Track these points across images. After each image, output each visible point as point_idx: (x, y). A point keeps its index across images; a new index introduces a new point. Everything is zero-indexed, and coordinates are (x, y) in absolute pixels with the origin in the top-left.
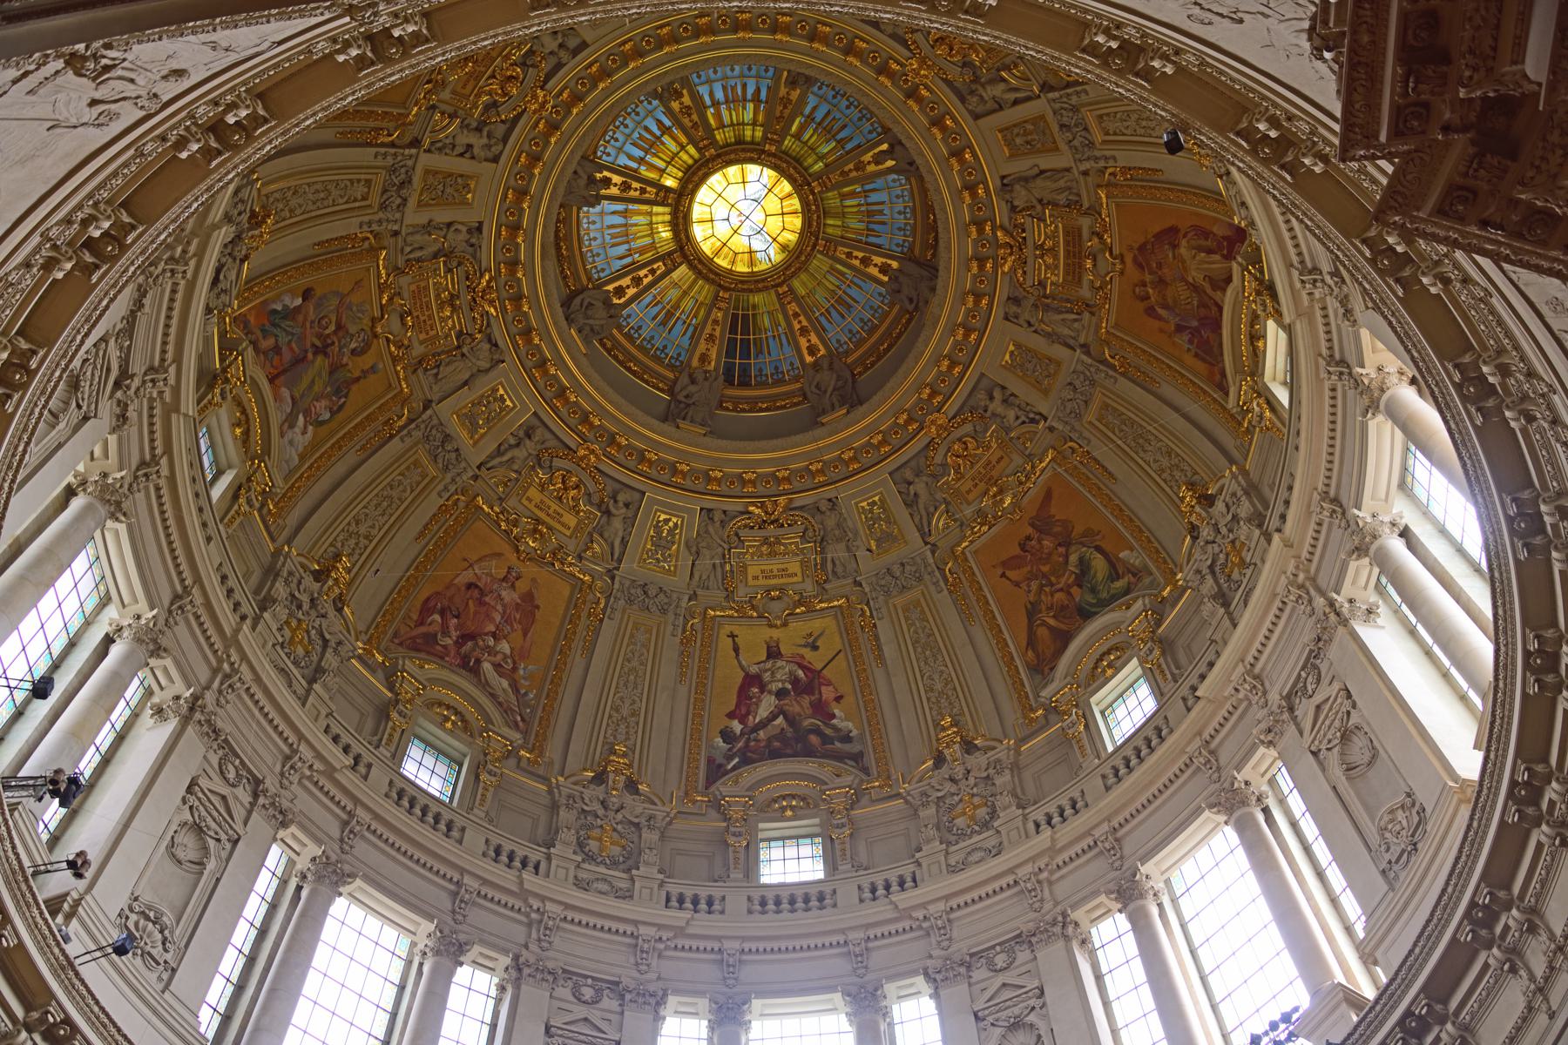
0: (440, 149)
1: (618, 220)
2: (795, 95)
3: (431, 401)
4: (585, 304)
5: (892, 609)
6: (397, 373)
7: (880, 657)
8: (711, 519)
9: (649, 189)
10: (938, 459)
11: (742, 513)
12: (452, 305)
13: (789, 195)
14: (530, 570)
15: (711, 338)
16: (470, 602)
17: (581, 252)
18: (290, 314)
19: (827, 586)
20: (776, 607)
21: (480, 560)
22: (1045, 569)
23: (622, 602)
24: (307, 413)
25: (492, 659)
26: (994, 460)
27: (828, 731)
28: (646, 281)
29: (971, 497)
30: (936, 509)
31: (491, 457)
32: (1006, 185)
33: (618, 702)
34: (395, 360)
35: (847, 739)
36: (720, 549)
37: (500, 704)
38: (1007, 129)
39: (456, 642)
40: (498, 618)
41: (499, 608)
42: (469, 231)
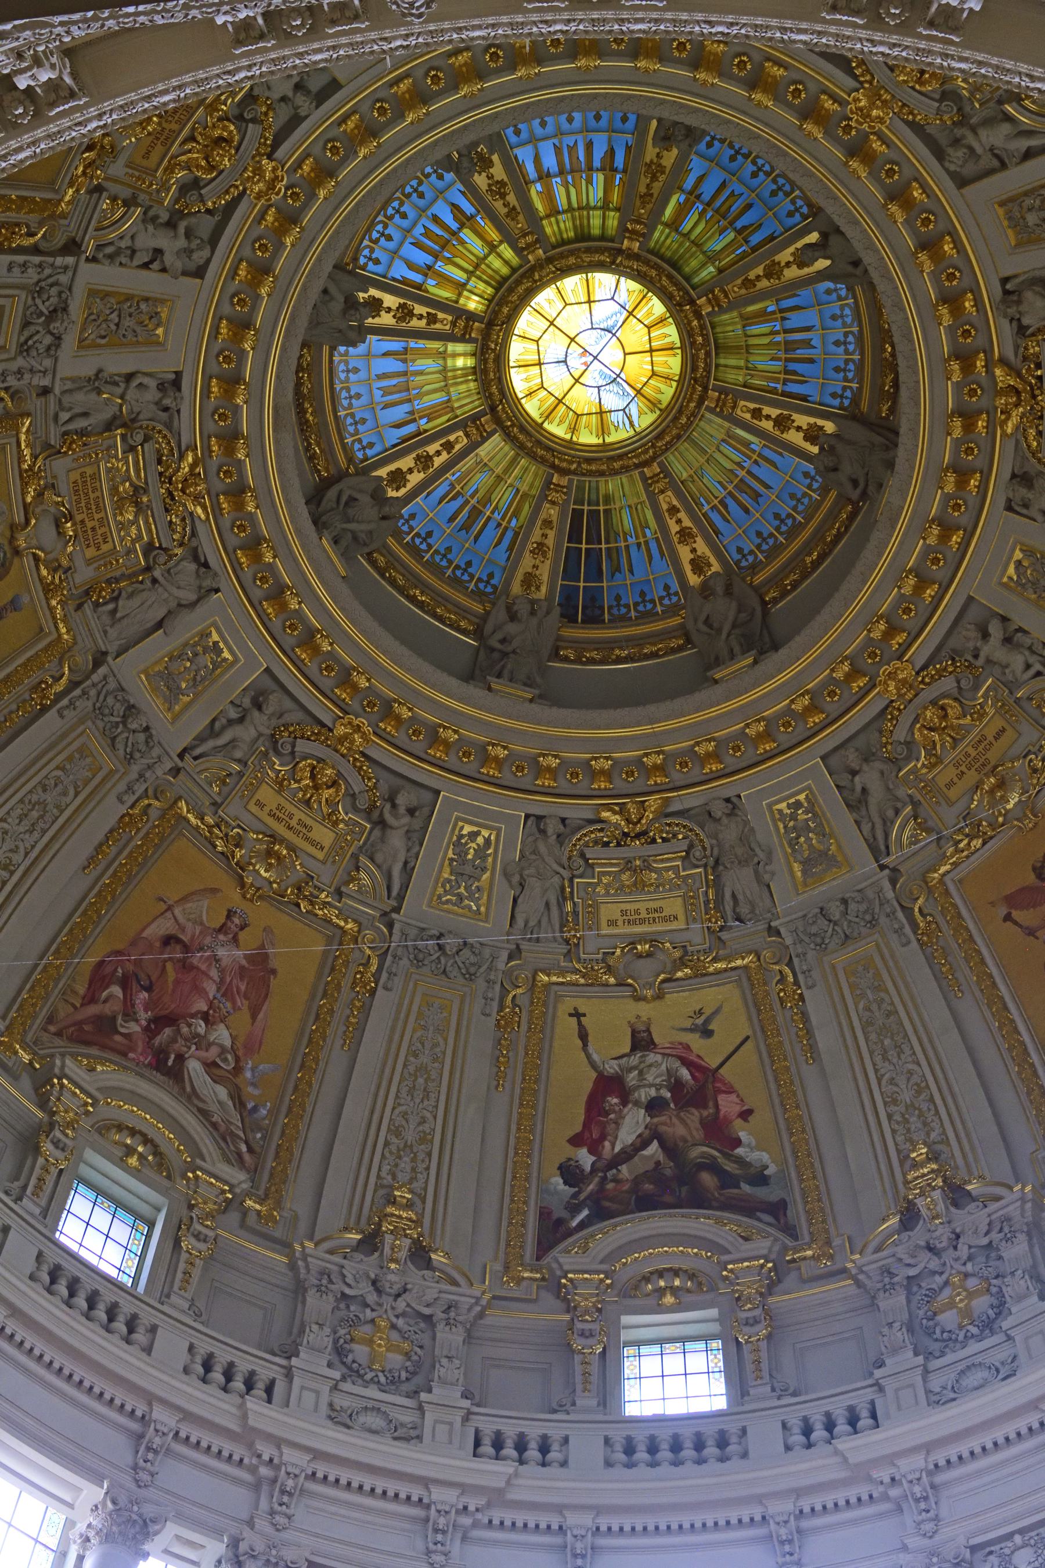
0: (111, 257)
1: (392, 365)
2: (670, 157)
3: (105, 654)
4: (344, 499)
5: (828, 970)
6: (52, 609)
8: (543, 832)
9: (441, 315)
10: (901, 734)
11: (591, 822)
12: (137, 504)
13: (662, 321)
14: (260, 914)
15: (540, 548)
16: (169, 966)
17: (337, 418)
19: (724, 935)
20: (646, 968)
21: (184, 899)
25: (202, 1054)
27: (729, 1167)
28: (438, 461)
29: (953, 794)
30: (897, 812)
31: (201, 739)
33: (399, 1121)
34: (48, 590)
35: (760, 1179)
36: (556, 879)
37: (215, 1125)
38: (1011, 200)
39: (146, 1029)
40: (211, 989)
41: (214, 973)
42: (161, 387)
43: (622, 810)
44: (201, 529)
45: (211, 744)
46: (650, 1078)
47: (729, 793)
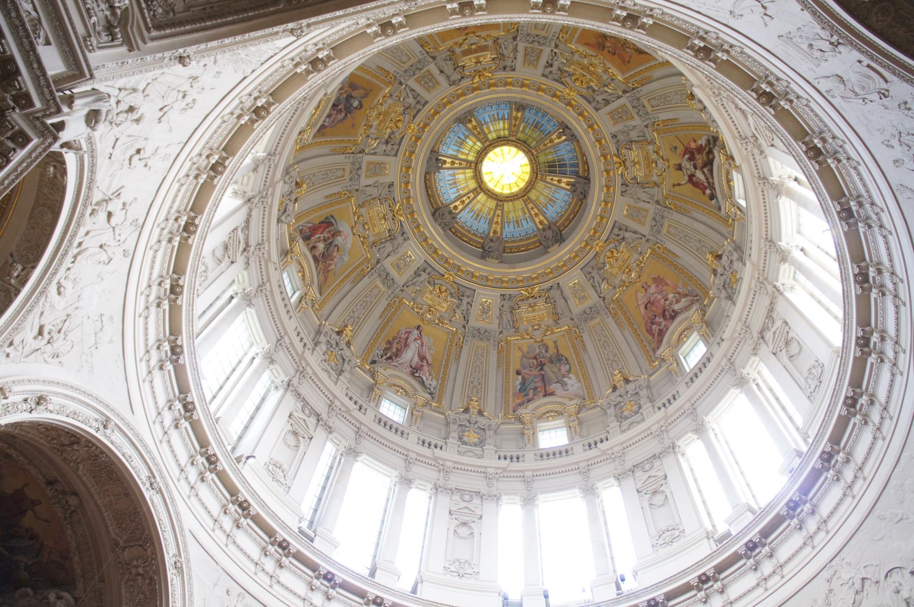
1: (511, 226)
7: (676, 119)
15: (559, 181)
18: (523, 383)
19: (649, 140)
21: (637, 300)
22: (619, 46)
23: (659, 237)
24: (564, 376)
26: (580, 67)
27: (707, 149)
30: (607, 92)
31: (596, 291)
32: (452, 83)
34: (552, 333)
35: (708, 140)
40: (660, 297)
41: (656, 295)
42: (504, 300)
43: (618, 168)
44: (542, 288)
45: (598, 289)
46: (688, 167)
47: (610, 136)
